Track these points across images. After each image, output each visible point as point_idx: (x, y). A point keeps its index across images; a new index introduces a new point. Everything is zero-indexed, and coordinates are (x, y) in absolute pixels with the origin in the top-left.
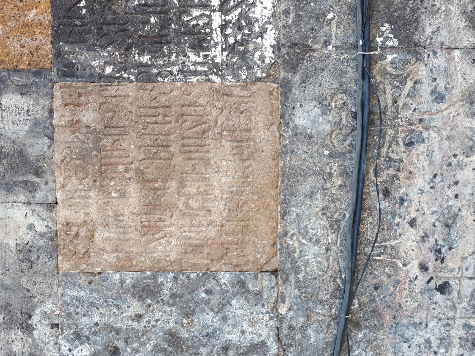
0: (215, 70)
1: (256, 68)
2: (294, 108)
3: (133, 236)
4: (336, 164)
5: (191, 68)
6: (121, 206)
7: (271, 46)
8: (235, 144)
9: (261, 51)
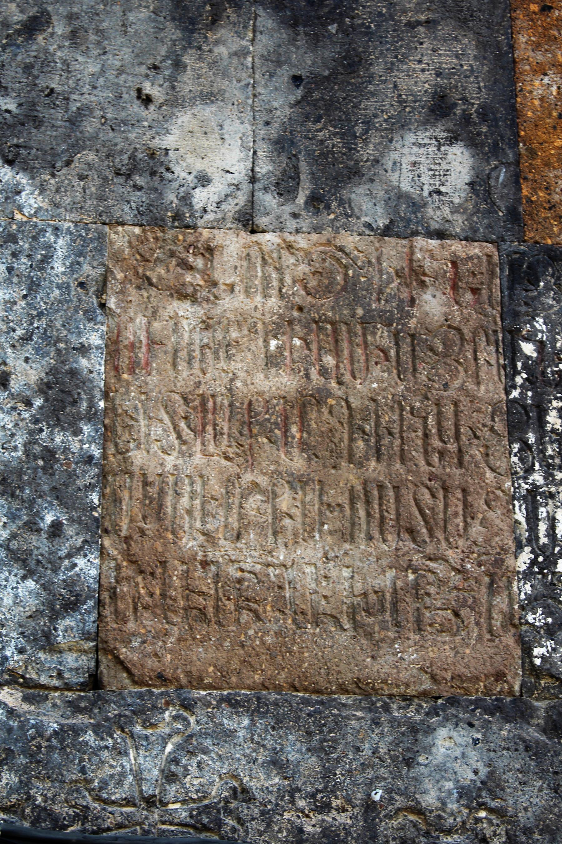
0: (541, 559)
1: (550, 644)
2: (471, 725)
3: (185, 376)
4: (349, 822)
5: (542, 509)
6: (249, 356)
8: (388, 597)
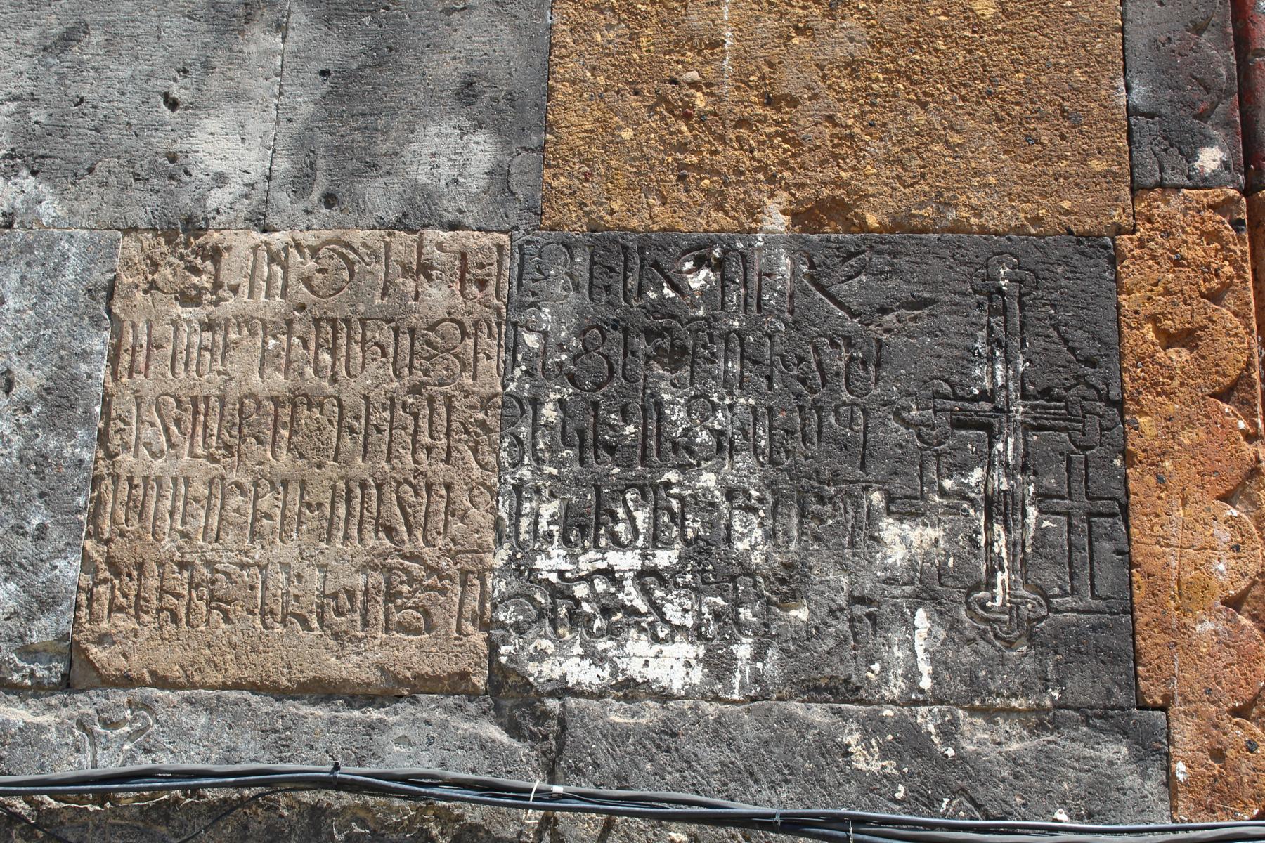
0: (519, 556)
4: (295, 818)
7: (564, 675)
9: (553, 655)
